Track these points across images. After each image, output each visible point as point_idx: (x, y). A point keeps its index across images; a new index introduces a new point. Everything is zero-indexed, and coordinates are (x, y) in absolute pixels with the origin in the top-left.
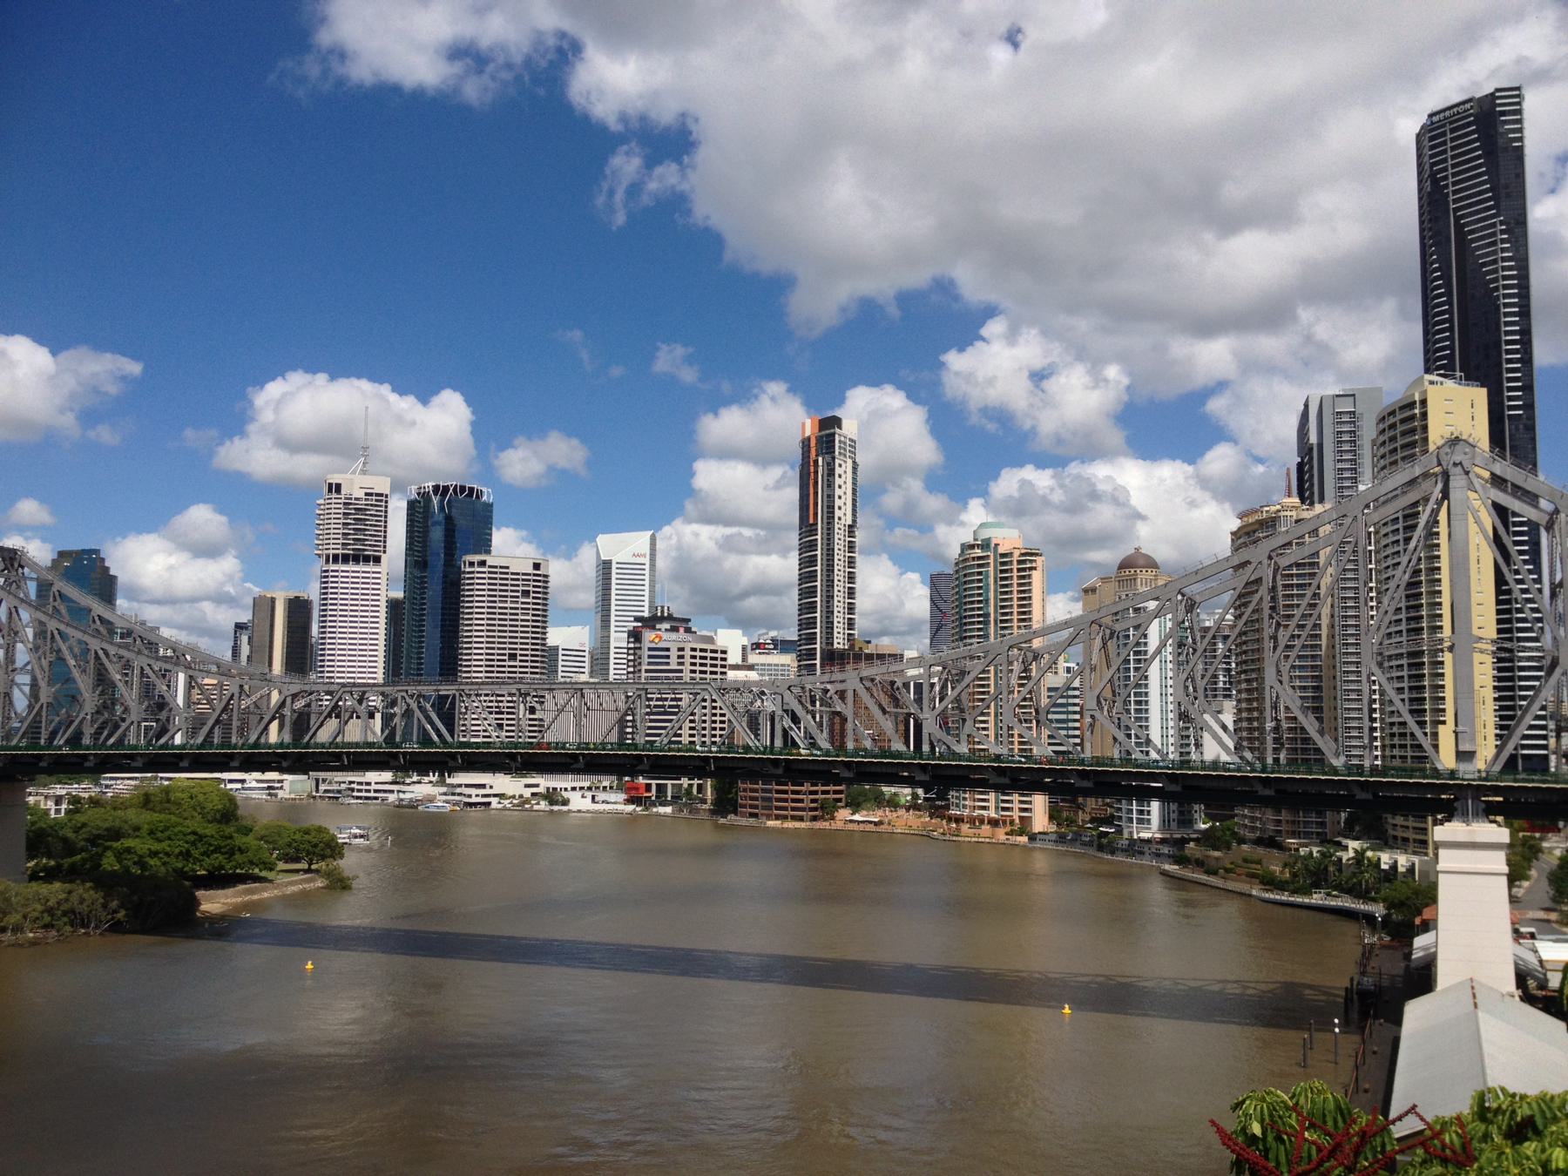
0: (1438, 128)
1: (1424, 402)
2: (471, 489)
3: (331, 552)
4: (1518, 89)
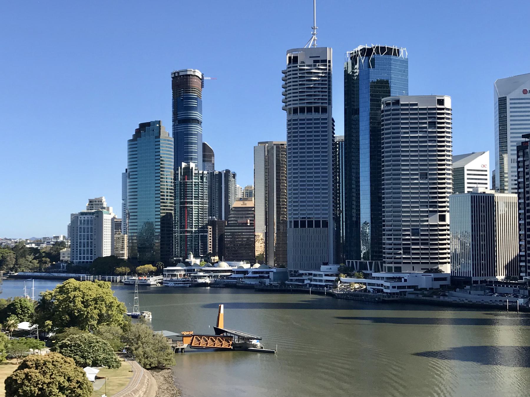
2: (390, 50)
3: (292, 106)
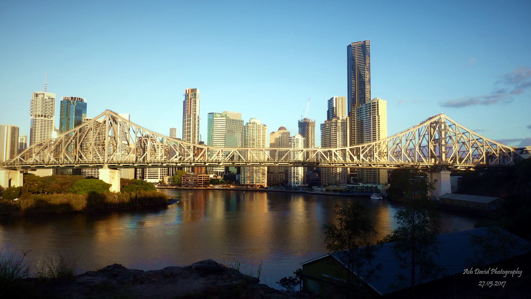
0: (354, 46)
1: (378, 102)
2: (82, 99)
3: (37, 114)
4: (369, 41)
